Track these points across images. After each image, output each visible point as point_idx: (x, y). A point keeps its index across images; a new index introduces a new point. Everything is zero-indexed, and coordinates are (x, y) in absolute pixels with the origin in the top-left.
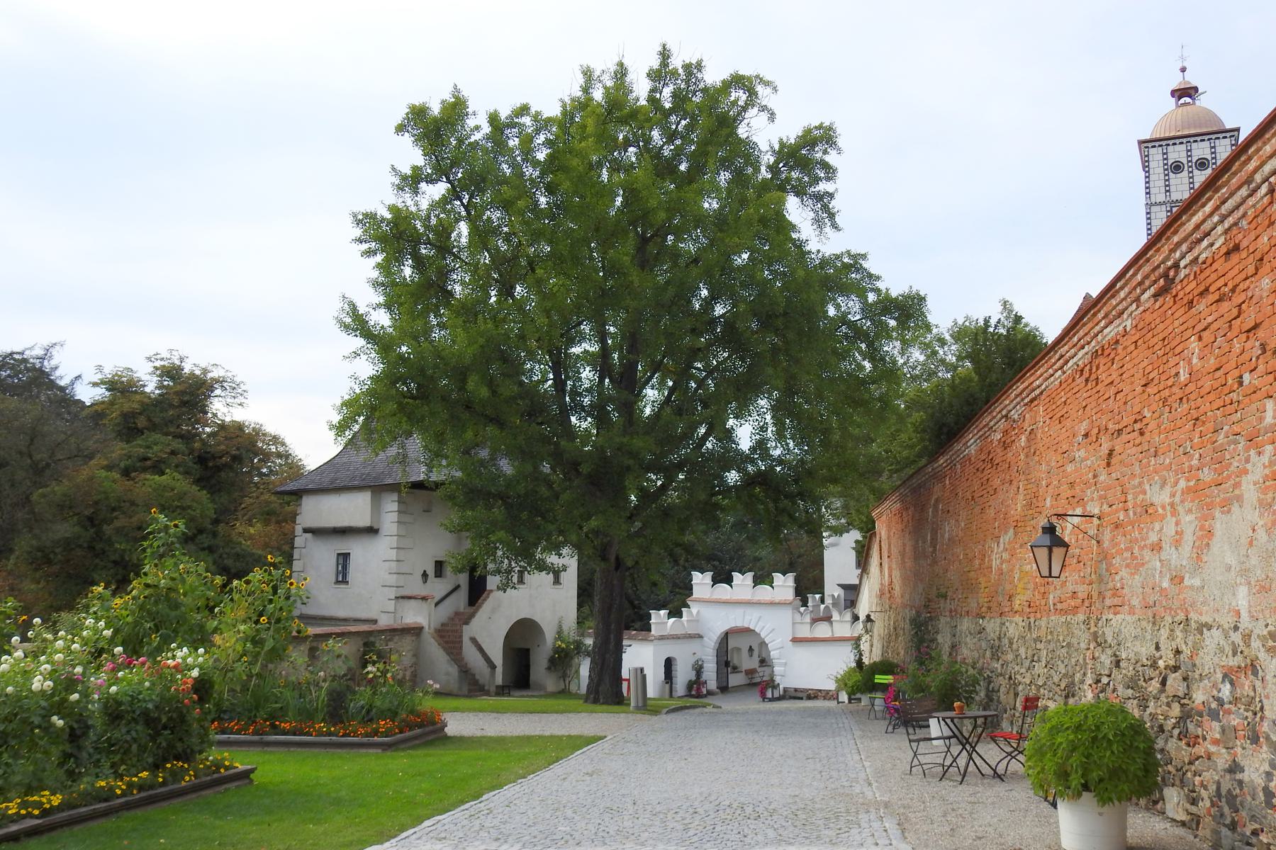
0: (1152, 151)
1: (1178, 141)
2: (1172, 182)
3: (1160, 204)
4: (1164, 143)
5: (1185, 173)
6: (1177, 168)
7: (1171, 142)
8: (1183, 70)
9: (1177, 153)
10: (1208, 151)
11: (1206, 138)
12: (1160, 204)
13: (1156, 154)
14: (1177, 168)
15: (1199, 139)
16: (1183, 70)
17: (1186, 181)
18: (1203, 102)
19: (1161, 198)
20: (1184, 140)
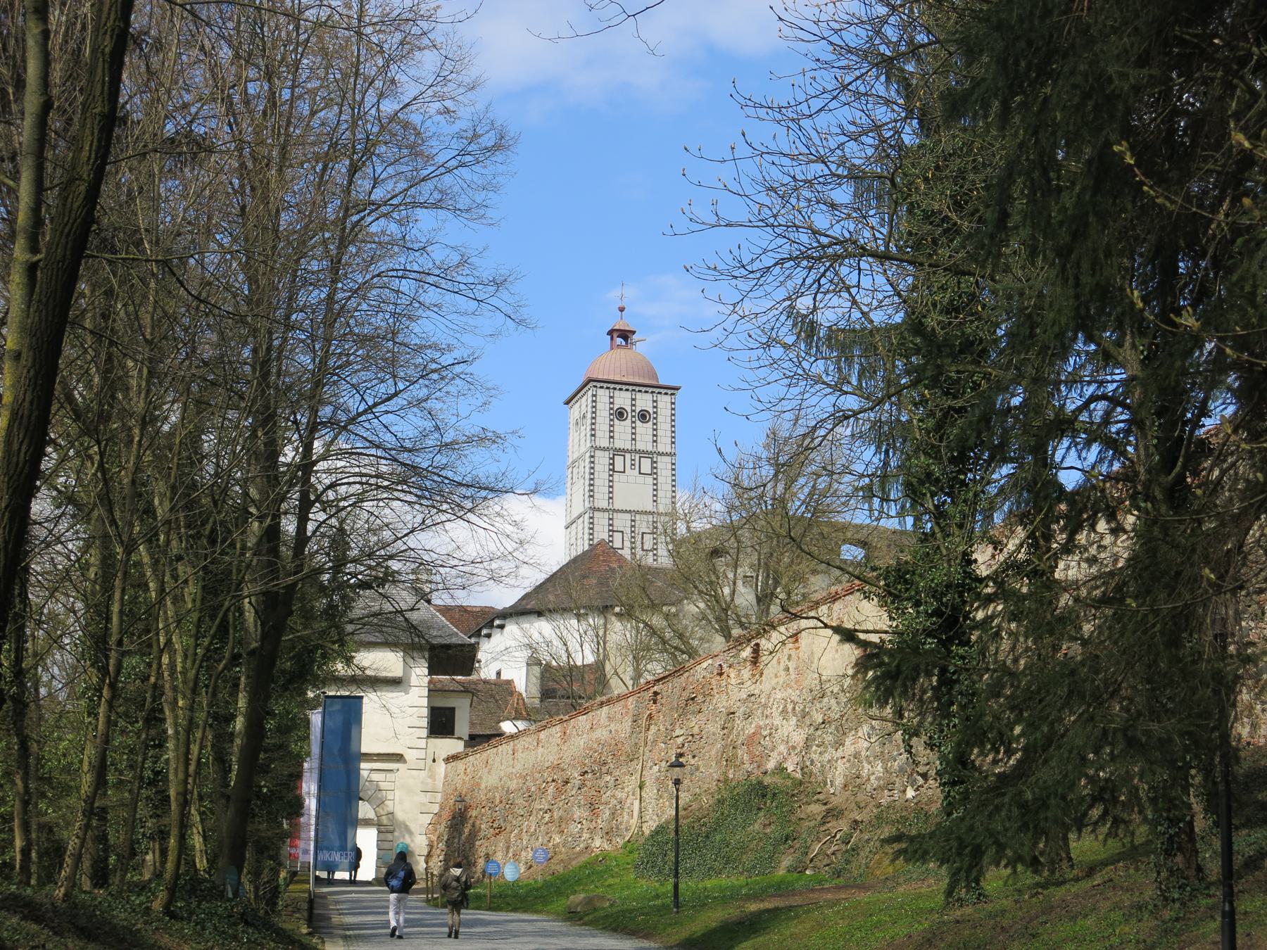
0: (600, 392)
1: (624, 387)
2: (616, 429)
3: (604, 449)
4: (612, 386)
5: (628, 422)
6: (620, 414)
7: (618, 387)
8: (622, 310)
9: (623, 400)
10: (650, 404)
11: (650, 390)
12: (604, 449)
13: (603, 395)
14: (620, 414)
15: (644, 389)
16: (622, 310)
17: (629, 430)
18: (640, 348)
19: (604, 442)
20: (630, 388)
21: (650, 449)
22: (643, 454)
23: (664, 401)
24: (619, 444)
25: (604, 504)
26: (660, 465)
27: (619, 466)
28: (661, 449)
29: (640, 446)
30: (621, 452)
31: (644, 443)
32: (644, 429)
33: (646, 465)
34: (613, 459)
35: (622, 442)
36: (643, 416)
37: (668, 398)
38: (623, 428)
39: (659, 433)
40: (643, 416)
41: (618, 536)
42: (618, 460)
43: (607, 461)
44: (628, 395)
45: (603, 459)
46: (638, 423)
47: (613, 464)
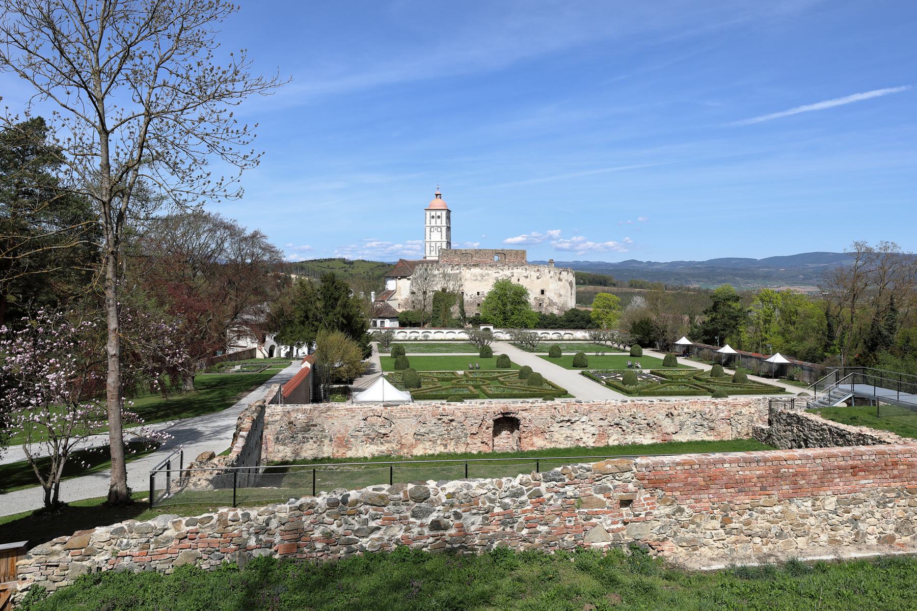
6: (433, 217)
9: (433, 213)
13: (428, 213)
22: (438, 227)
24: (432, 225)
25: (429, 240)
29: (438, 225)
31: (439, 224)
33: (439, 229)
35: (433, 224)
36: (439, 217)
38: (433, 221)
40: (439, 217)
41: (432, 248)
42: (432, 229)
45: (428, 229)
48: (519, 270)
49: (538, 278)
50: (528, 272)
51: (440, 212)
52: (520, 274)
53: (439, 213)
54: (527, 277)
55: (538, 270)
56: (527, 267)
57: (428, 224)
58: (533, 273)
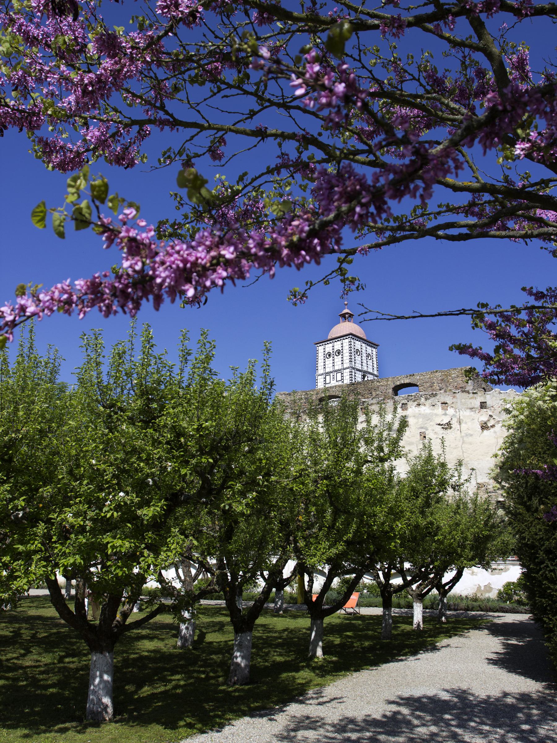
5: (331, 358)
9: (329, 348)
10: (340, 346)
13: (321, 349)
21: (340, 368)
23: (346, 342)
24: (328, 370)
26: (345, 374)
27: (328, 381)
28: (345, 366)
29: (336, 368)
30: (328, 374)
32: (338, 359)
33: (339, 375)
34: (325, 378)
37: (347, 340)
38: (329, 361)
39: (344, 358)
40: (339, 352)
42: (328, 377)
43: (323, 380)
44: (331, 345)
46: (335, 357)
47: (325, 381)
48: (425, 409)
49: (484, 427)
50: (451, 411)
51: (339, 343)
52: (428, 418)
53: (337, 345)
54: (448, 426)
55: (483, 405)
56: (448, 399)
57: (321, 370)
58: (465, 414)
